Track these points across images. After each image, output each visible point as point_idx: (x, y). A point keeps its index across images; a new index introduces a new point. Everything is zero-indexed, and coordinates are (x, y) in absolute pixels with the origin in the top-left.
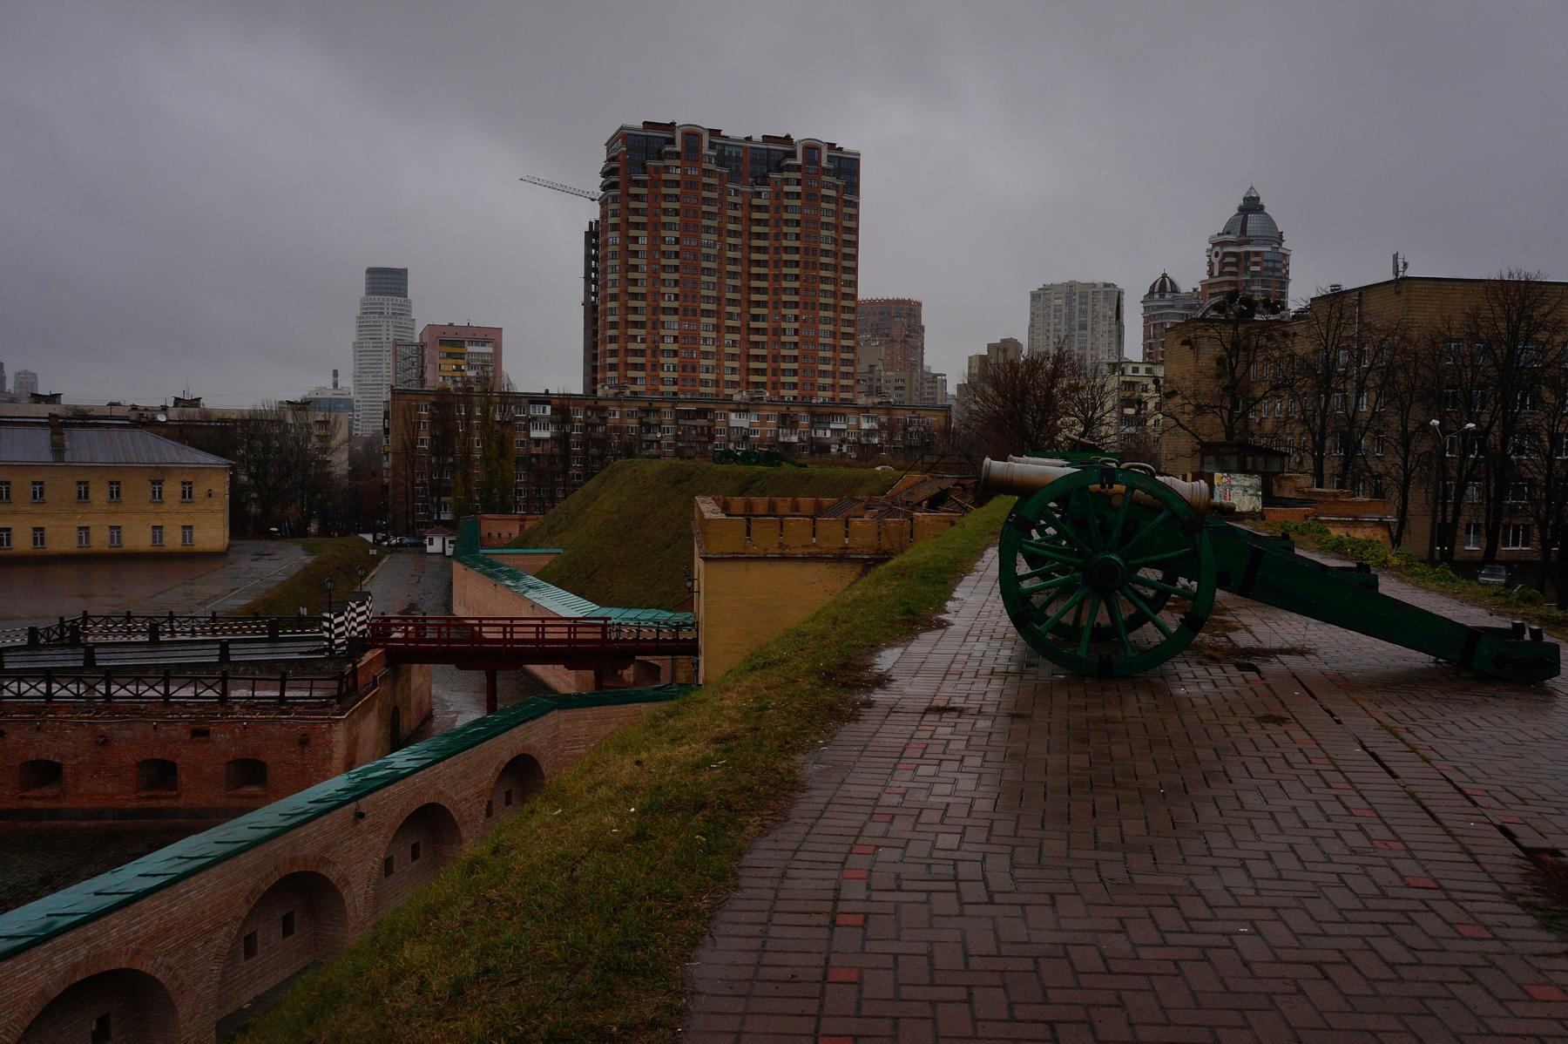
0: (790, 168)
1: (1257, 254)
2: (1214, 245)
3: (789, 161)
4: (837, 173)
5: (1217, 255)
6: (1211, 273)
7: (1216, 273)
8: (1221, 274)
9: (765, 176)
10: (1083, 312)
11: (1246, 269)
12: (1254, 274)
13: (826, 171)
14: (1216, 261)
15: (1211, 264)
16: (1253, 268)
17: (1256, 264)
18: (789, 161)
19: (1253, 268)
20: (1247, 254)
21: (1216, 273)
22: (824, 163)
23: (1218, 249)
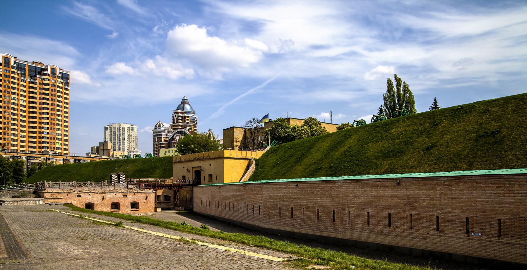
0: (44, 74)
1: (188, 117)
2: (174, 113)
3: (45, 72)
4: (62, 78)
5: (176, 116)
6: (174, 123)
7: (176, 122)
8: (177, 122)
9: (35, 76)
10: (124, 134)
11: (185, 121)
12: (187, 123)
13: (59, 77)
14: (175, 118)
15: (174, 120)
16: (187, 121)
17: (188, 120)
18: (45, 72)
19: (187, 121)
20: (185, 116)
21: (176, 122)
22: (58, 74)
23: (176, 114)
